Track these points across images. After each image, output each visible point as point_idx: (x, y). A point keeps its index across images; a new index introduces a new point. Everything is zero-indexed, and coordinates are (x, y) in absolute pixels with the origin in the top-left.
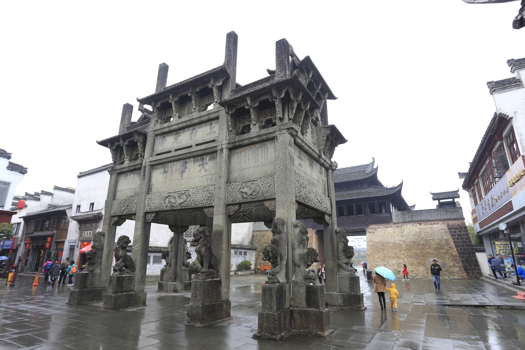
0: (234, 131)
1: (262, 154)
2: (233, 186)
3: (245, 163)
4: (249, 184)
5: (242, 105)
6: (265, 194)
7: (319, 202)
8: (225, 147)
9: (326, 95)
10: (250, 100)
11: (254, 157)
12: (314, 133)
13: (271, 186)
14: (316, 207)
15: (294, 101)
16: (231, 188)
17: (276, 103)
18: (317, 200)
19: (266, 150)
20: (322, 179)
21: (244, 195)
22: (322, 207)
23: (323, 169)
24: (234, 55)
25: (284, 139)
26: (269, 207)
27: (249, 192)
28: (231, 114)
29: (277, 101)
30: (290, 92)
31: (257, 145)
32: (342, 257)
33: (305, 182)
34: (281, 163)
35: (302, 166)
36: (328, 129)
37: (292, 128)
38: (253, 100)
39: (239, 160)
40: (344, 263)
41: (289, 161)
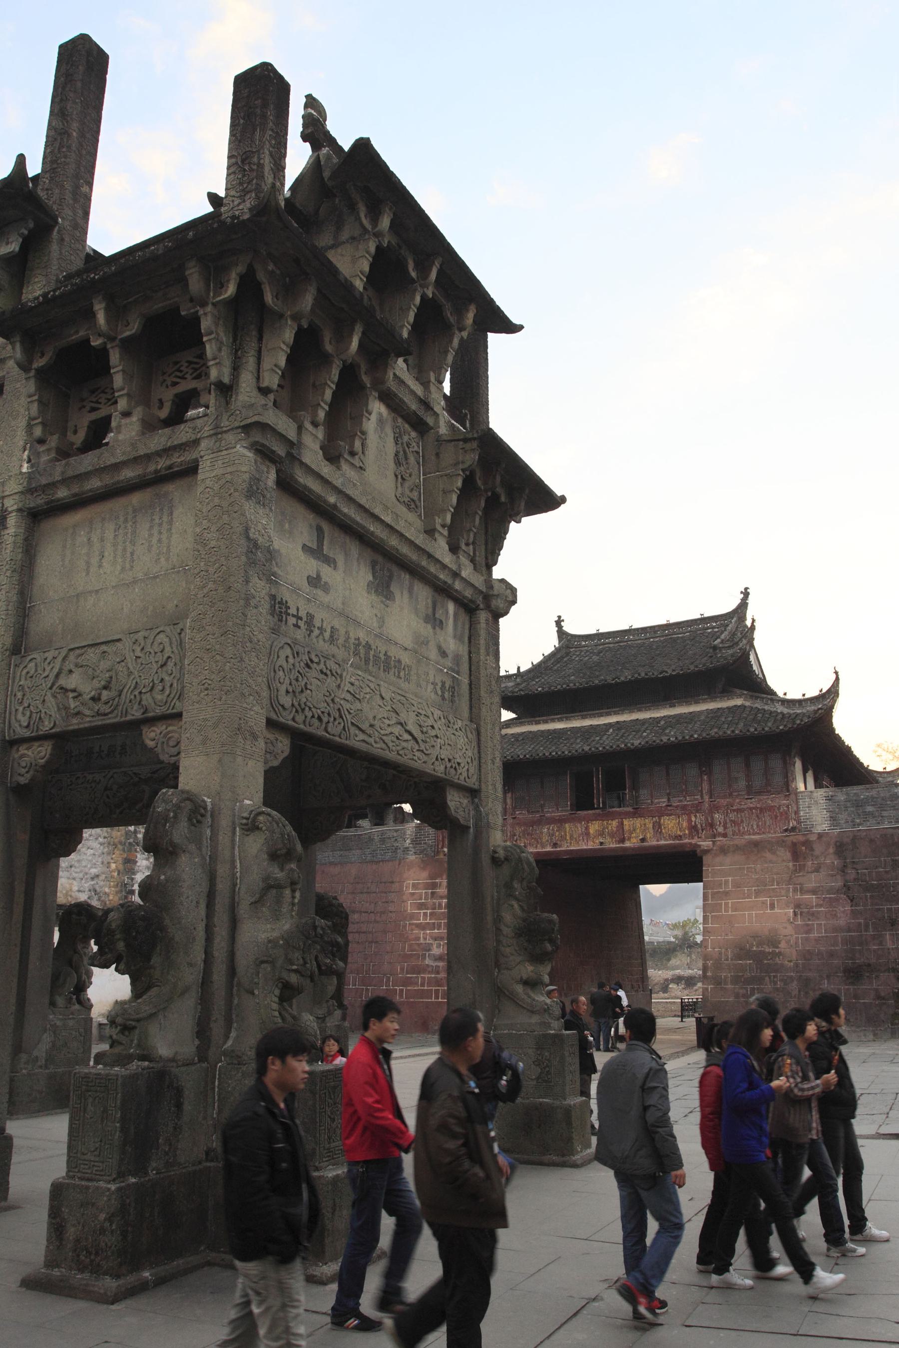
0: (53, 441)
1: (151, 535)
2: (32, 665)
3: (88, 574)
4: (92, 656)
5: (82, 333)
6: (144, 697)
7: (406, 736)
8: (15, 507)
9: (468, 311)
10: (107, 310)
11: (119, 553)
12: (412, 459)
13: (170, 664)
14: (392, 756)
15: (281, 316)
16: (25, 672)
17: (206, 324)
18: (397, 730)
19: (165, 519)
20: (439, 648)
21: (71, 700)
22: (425, 758)
23: (451, 607)
24: (82, 135)
25: (229, 469)
26: (159, 749)
27: (88, 689)
28: (39, 371)
29: (205, 314)
30: (261, 276)
31: (136, 498)
32: (511, 958)
33: (341, 654)
34: (212, 570)
35: (326, 588)
36: (468, 446)
37: (264, 427)
38: (116, 313)
39: (67, 562)
40: (517, 982)
41: (244, 558)
